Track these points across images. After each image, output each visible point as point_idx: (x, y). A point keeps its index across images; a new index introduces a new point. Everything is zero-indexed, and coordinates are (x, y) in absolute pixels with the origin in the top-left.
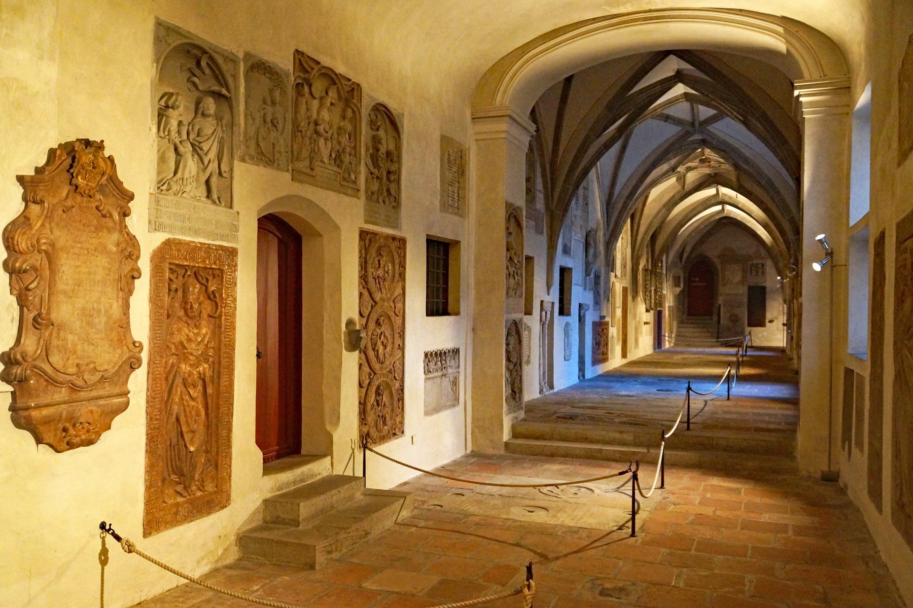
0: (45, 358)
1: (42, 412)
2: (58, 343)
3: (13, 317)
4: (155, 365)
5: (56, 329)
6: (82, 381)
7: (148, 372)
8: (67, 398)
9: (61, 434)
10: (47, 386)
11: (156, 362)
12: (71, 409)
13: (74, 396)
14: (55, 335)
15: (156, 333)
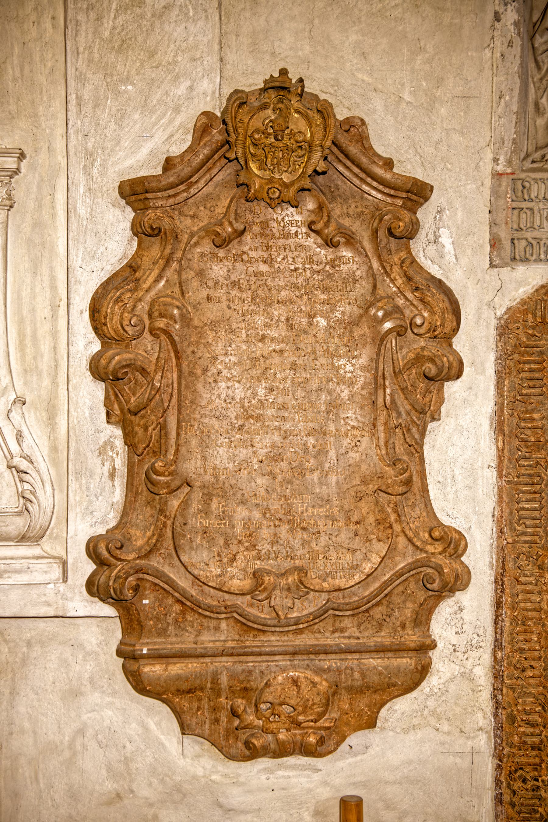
0: (174, 552)
1: (170, 668)
2: (205, 523)
3: (114, 469)
4: (519, 588)
5: (197, 495)
6: (267, 609)
7: (498, 604)
8: (230, 644)
9: (229, 721)
10: (183, 613)
11: (523, 579)
12: (239, 668)
13: (250, 642)
14: (195, 505)
15: (523, 509)
